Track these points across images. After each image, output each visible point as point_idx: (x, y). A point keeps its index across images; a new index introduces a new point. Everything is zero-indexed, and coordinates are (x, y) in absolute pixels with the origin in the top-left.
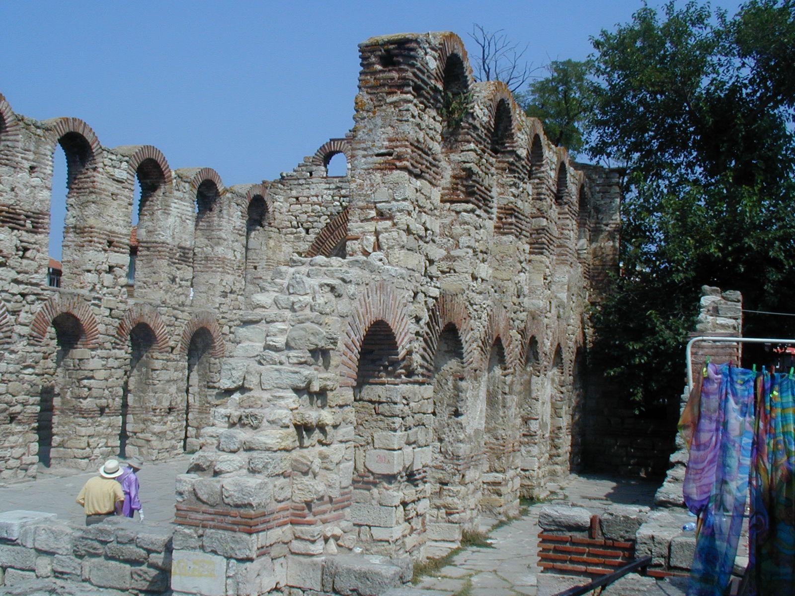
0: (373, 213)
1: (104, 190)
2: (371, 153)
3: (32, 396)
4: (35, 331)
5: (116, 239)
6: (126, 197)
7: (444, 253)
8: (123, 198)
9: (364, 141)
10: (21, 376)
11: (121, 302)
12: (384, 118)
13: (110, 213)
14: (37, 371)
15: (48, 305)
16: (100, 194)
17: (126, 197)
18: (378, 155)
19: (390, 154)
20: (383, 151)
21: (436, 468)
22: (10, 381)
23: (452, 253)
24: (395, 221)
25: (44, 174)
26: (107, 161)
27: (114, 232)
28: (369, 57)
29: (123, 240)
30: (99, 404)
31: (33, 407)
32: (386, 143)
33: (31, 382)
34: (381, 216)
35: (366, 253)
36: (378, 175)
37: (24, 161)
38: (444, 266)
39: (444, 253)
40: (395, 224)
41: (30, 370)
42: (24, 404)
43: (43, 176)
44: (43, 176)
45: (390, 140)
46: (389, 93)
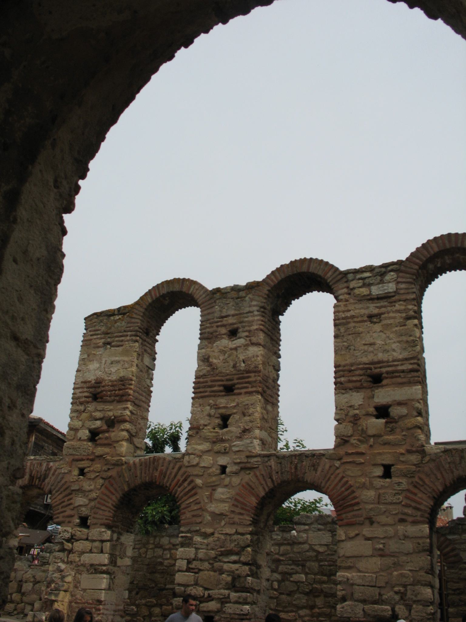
1: (353, 317)
3: (236, 592)
4: (237, 506)
5: (384, 370)
6: (399, 311)
8: (391, 315)
10: (216, 564)
11: (409, 452)
13: (368, 339)
14: (242, 559)
15: (258, 474)
16: (349, 323)
17: (399, 311)
22: (200, 570)
25: (249, 331)
26: (352, 285)
27: (379, 362)
29: (400, 368)
30: (370, 612)
31: (237, 606)
33: (233, 572)
37: (219, 329)
41: (234, 558)
42: (224, 601)
43: (247, 334)
44: (247, 334)
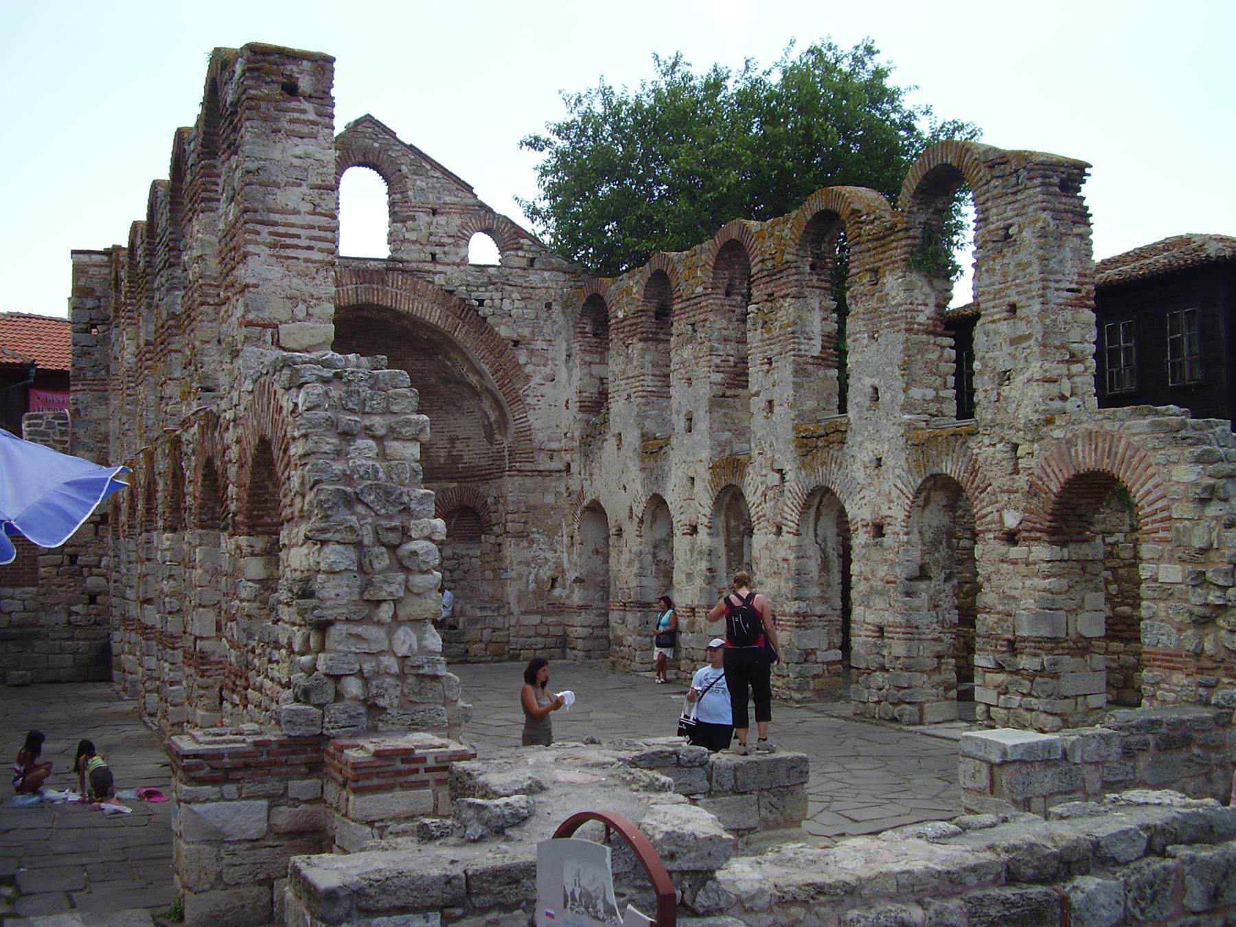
0: (1067, 357)
2: (1062, 285)
7: (934, 393)
9: (1055, 273)
12: (1074, 250)
18: (1068, 290)
19: (1079, 291)
20: (1074, 286)
21: (934, 640)
23: (942, 393)
24: (1088, 364)
28: (1052, 177)
32: (1076, 278)
34: (1074, 358)
35: (1063, 398)
36: (1068, 314)
38: (933, 408)
39: (934, 393)
40: (1086, 369)
45: (1080, 275)
46: (1074, 223)
